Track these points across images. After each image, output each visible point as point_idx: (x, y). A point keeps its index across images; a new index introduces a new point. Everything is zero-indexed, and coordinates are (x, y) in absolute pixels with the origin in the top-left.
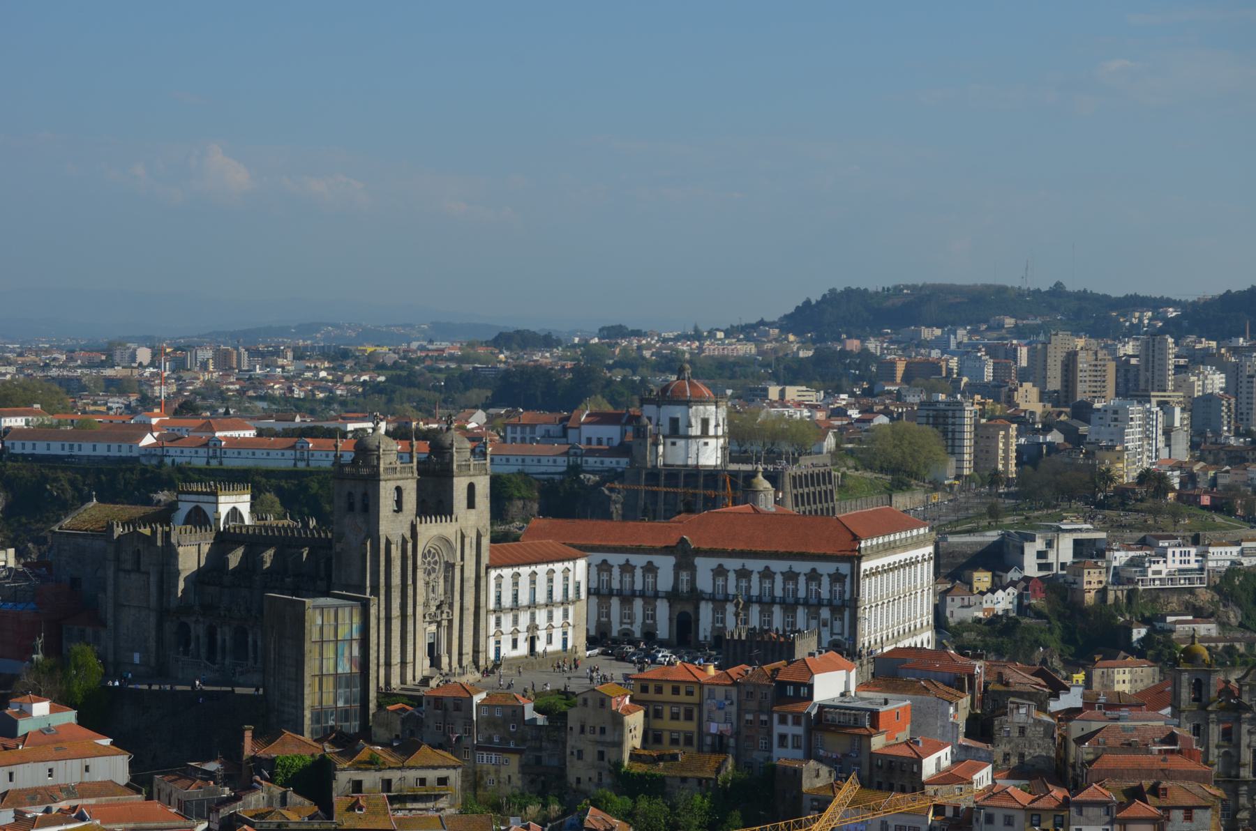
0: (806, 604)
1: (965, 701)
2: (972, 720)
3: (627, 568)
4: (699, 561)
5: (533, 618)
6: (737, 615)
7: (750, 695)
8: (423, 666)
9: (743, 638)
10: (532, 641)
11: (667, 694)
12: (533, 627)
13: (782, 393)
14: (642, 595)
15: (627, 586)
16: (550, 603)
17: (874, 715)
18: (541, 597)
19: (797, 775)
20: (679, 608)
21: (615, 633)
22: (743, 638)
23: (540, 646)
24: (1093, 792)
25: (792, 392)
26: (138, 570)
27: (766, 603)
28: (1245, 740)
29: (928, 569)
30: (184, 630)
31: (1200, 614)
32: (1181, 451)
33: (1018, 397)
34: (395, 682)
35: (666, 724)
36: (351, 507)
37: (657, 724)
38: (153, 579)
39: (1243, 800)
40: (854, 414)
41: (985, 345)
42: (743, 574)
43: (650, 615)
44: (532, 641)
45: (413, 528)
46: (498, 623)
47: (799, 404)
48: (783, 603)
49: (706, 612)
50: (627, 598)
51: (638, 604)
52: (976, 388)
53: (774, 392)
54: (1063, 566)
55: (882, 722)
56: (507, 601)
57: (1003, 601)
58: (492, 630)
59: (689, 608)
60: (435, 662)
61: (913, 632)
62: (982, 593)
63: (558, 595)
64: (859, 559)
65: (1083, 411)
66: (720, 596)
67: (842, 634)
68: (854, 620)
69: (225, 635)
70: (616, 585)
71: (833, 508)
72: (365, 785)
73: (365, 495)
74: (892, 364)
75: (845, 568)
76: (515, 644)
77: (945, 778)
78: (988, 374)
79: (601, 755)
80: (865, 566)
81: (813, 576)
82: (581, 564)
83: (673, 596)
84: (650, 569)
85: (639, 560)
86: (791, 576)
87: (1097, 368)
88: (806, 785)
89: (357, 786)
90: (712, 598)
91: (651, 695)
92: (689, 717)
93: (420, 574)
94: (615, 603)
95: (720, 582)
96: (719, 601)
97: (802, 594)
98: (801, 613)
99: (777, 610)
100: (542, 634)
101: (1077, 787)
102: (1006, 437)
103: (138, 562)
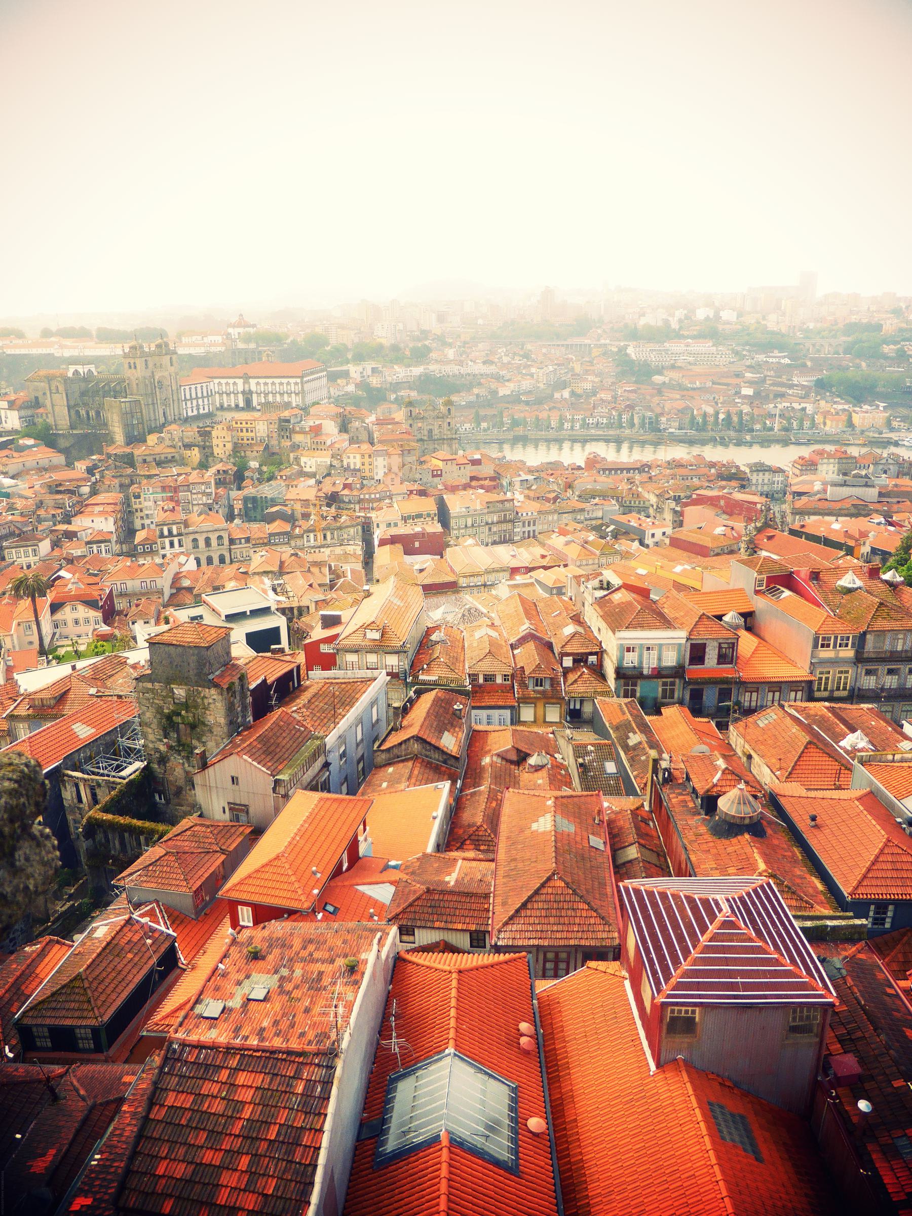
3: (227, 384)
8: (162, 420)
10: (198, 409)
11: (244, 425)
12: (198, 405)
16: (203, 397)
18: (199, 395)
26: (58, 392)
29: (325, 379)
30: (78, 412)
31: (410, 388)
34: (153, 426)
35: (244, 434)
36: (130, 367)
37: (241, 434)
38: (64, 395)
42: (266, 384)
44: (198, 409)
45: (153, 373)
48: (279, 393)
49: (255, 396)
50: (228, 394)
51: (232, 395)
56: (188, 397)
57: (351, 388)
63: (205, 394)
69: (92, 413)
72: (148, 460)
75: (299, 380)
80: (305, 379)
81: (288, 383)
83: (243, 392)
84: (235, 383)
85: (231, 381)
86: (281, 384)
89: (145, 461)
91: (239, 425)
92: (252, 431)
94: (225, 395)
96: (258, 394)
98: (286, 395)
103: (57, 389)
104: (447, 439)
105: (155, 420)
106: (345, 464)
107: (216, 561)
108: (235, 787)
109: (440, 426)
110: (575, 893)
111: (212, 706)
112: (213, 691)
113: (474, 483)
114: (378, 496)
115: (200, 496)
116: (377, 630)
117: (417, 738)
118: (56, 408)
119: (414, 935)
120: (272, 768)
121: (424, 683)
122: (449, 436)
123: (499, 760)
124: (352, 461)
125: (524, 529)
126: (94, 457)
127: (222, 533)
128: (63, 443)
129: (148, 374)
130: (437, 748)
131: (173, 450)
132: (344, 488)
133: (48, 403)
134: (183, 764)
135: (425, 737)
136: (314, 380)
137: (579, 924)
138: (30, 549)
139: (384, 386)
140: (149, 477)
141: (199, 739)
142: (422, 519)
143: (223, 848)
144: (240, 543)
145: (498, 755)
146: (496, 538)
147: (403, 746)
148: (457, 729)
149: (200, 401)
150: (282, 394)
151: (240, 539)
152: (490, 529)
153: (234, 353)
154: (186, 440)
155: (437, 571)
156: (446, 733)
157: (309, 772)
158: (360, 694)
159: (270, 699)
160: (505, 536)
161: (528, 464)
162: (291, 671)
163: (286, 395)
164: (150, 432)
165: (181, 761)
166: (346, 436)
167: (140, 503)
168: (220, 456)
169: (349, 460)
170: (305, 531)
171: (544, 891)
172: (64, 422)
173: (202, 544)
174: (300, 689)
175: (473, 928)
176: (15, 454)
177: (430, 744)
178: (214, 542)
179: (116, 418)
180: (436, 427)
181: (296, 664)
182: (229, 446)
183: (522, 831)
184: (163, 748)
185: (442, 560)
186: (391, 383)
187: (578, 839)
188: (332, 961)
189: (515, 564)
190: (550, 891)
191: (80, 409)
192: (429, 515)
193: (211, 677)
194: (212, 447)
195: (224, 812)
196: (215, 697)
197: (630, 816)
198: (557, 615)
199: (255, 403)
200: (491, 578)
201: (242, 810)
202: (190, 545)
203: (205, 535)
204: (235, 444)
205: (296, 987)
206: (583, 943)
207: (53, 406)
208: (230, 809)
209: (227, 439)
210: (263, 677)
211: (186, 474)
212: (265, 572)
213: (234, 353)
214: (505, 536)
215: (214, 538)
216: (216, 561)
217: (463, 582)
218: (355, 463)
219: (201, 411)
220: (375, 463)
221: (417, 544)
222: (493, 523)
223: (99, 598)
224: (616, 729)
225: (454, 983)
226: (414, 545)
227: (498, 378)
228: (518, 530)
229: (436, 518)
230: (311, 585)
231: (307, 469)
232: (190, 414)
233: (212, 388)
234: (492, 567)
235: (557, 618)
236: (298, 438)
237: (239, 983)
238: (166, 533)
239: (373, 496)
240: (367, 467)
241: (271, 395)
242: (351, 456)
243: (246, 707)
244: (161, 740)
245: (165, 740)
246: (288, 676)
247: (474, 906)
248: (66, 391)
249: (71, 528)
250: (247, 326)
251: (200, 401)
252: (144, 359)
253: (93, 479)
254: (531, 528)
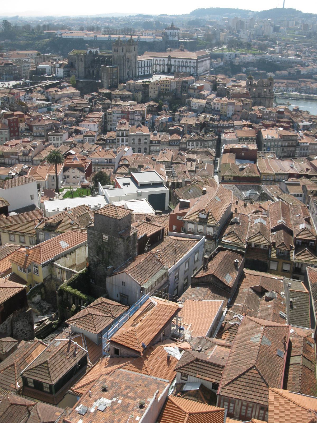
0: (189, 67)
3: (160, 60)
4: (172, 59)
5: (144, 69)
6: (177, 69)
7: (178, 83)
8: (127, 76)
10: (144, 72)
12: (144, 70)
14: (162, 65)
15: (160, 63)
16: (147, 66)
18: (146, 65)
20: (168, 67)
21: (158, 71)
23: (146, 73)
27: (182, 66)
30: (89, 70)
34: (122, 79)
35: (165, 87)
36: (115, 51)
37: (163, 87)
38: (84, 62)
42: (179, 62)
43: (164, 68)
44: (144, 72)
45: (125, 54)
46: (139, 70)
48: (185, 66)
49: (173, 67)
50: (160, 65)
51: (162, 66)
54: (233, 58)
56: (140, 66)
58: (138, 71)
59: (170, 67)
60: (128, 76)
61: (206, 71)
63: (149, 65)
66: (175, 65)
68: (197, 70)
70: (158, 63)
73: (117, 49)
76: (141, 73)
79: (154, 92)
80: (199, 61)
81: (190, 62)
82: (152, 60)
83: (167, 65)
84: (164, 60)
85: (162, 59)
86: (186, 62)
90: (174, 65)
92: (168, 86)
93: (126, 62)
94: (158, 66)
95: (175, 63)
96: (175, 66)
97: (188, 65)
98: (188, 68)
99: (184, 68)
100: (146, 71)
104: (268, 98)
105: (123, 76)
106: (213, 107)
107: (142, 150)
108: (123, 286)
110: (262, 378)
111: (119, 246)
112: (120, 239)
113: (277, 124)
114: (227, 125)
115: (139, 117)
116: (205, 214)
117: (212, 275)
118: (80, 68)
119: (187, 377)
120: (141, 281)
121: (224, 244)
122: (269, 97)
123: (252, 291)
124: (216, 106)
125: (301, 151)
126: (93, 93)
127: (147, 137)
128: (80, 85)
129: (123, 54)
130: (221, 282)
131: (130, 93)
132: (210, 120)
133: (76, 66)
134: (104, 269)
135: (216, 275)
137: (261, 393)
138: (59, 137)
139: (240, 64)
140: (117, 105)
141: (112, 259)
142: (248, 141)
143: (114, 315)
144: (155, 143)
145: (252, 288)
146: (285, 154)
147: (206, 278)
148: (234, 273)
149: (146, 68)
150: (186, 67)
151: (155, 141)
152: (283, 150)
153: (167, 42)
154: (136, 88)
155: (252, 169)
156: (228, 274)
157: (158, 285)
158: (190, 247)
159: (145, 246)
160: (290, 154)
161: (311, 113)
162: (159, 231)
163: (188, 68)
164: (121, 82)
165: (103, 267)
167: (111, 118)
168: (151, 97)
169: (215, 106)
170: (188, 141)
171: (248, 374)
172: (82, 75)
173: (137, 141)
174: (162, 240)
175: (214, 381)
176: (59, 90)
177: (218, 279)
178: (143, 141)
179: (105, 75)
181: (162, 228)
182: (157, 93)
183: (246, 340)
184: (96, 260)
185: (254, 165)
186: (244, 63)
187: (271, 349)
188: (135, 399)
189: (292, 171)
190: (250, 374)
191: (90, 69)
192: (252, 139)
193: (119, 233)
194: (148, 93)
195: (118, 296)
196: (121, 242)
197: (302, 340)
198: (298, 216)
199: (172, 71)
200: (277, 178)
201: (126, 297)
202: (131, 141)
203: (139, 138)
204: (160, 91)
205: (118, 408)
206: (260, 402)
207: (78, 67)
208: (121, 296)
209: (155, 89)
210: (145, 233)
211: (134, 105)
212: (164, 161)
213: (167, 42)
214: (290, 154)
215: (143, 139)
216: (142, 150)
217: (263, 178)
218: (218, 108)
219: (146, 73)
220: (228, 109)
221: (243, 154)
222: (285, 146)
223: (85, 166)
224: (313, 286)
225: (186, 419)
226: (241, 154)
227: (303, 65)
228: (298, 151)
229: (255, 141)
230: (185, 172)
231: (194, 108)
232: (140, 74)
233: (152, 62)
234: (279, 172)
235: (298, 218)
236: (191, 91)
237: (96, 401)
238: (120, 134)
239: (225, 125)
240: (223, 110)
241: (181, 67)
242: (216, 104)
243: (135, 248)
244: (95, 257)
245: (97, 257)
246: (158, 234)
247: (216, 371)
248: (85, 60)
249: (78, 128)
250: (175, 29)
251: (146, 68)
252: (122, 47)
253: (91, 104)
254: (305, 151)
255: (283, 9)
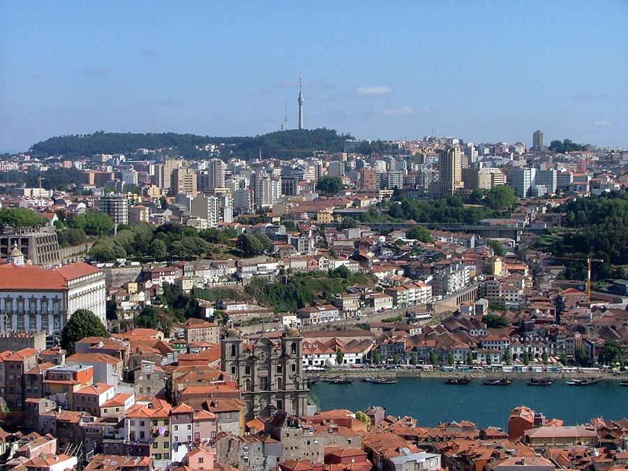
1: (120, 364)
2: (125, 372)
7: (12, 367)
9: (8, 337)
13: (32, 192)
17: (75, 375)
19: (36, 405)
22: (8, 337)
24: (183, 407)
25: (37, 191)
28: (256, 373)
32: (228, 218)
33: (150, 193)
39: (256, 402)
40: (69, 203)
41: (133, 164)
47: (39, 198)
52: (130, 187)
53: (27, 192)
55: (78, 376)
62: (133, 294)
64: (67, 290)
65: (182, 199)
67: (60, 328)
71: (58, 253)
74: (88, 175)
75: (60, 296)
77: (112, 403)
78: (135, 181)
80: (71, 293)
81: (44, 300)
86: (33, 300)
87: (188, 178)
88: (41, 412)
99: (27, 317)
101: (175, 405)
102: (144, 213)
109: (279, 369)
136: (83, 294)
166: (127, 389)
180: (274, 372)
220: (175, 434)
241: (15, 317)
255: (301, 131)
